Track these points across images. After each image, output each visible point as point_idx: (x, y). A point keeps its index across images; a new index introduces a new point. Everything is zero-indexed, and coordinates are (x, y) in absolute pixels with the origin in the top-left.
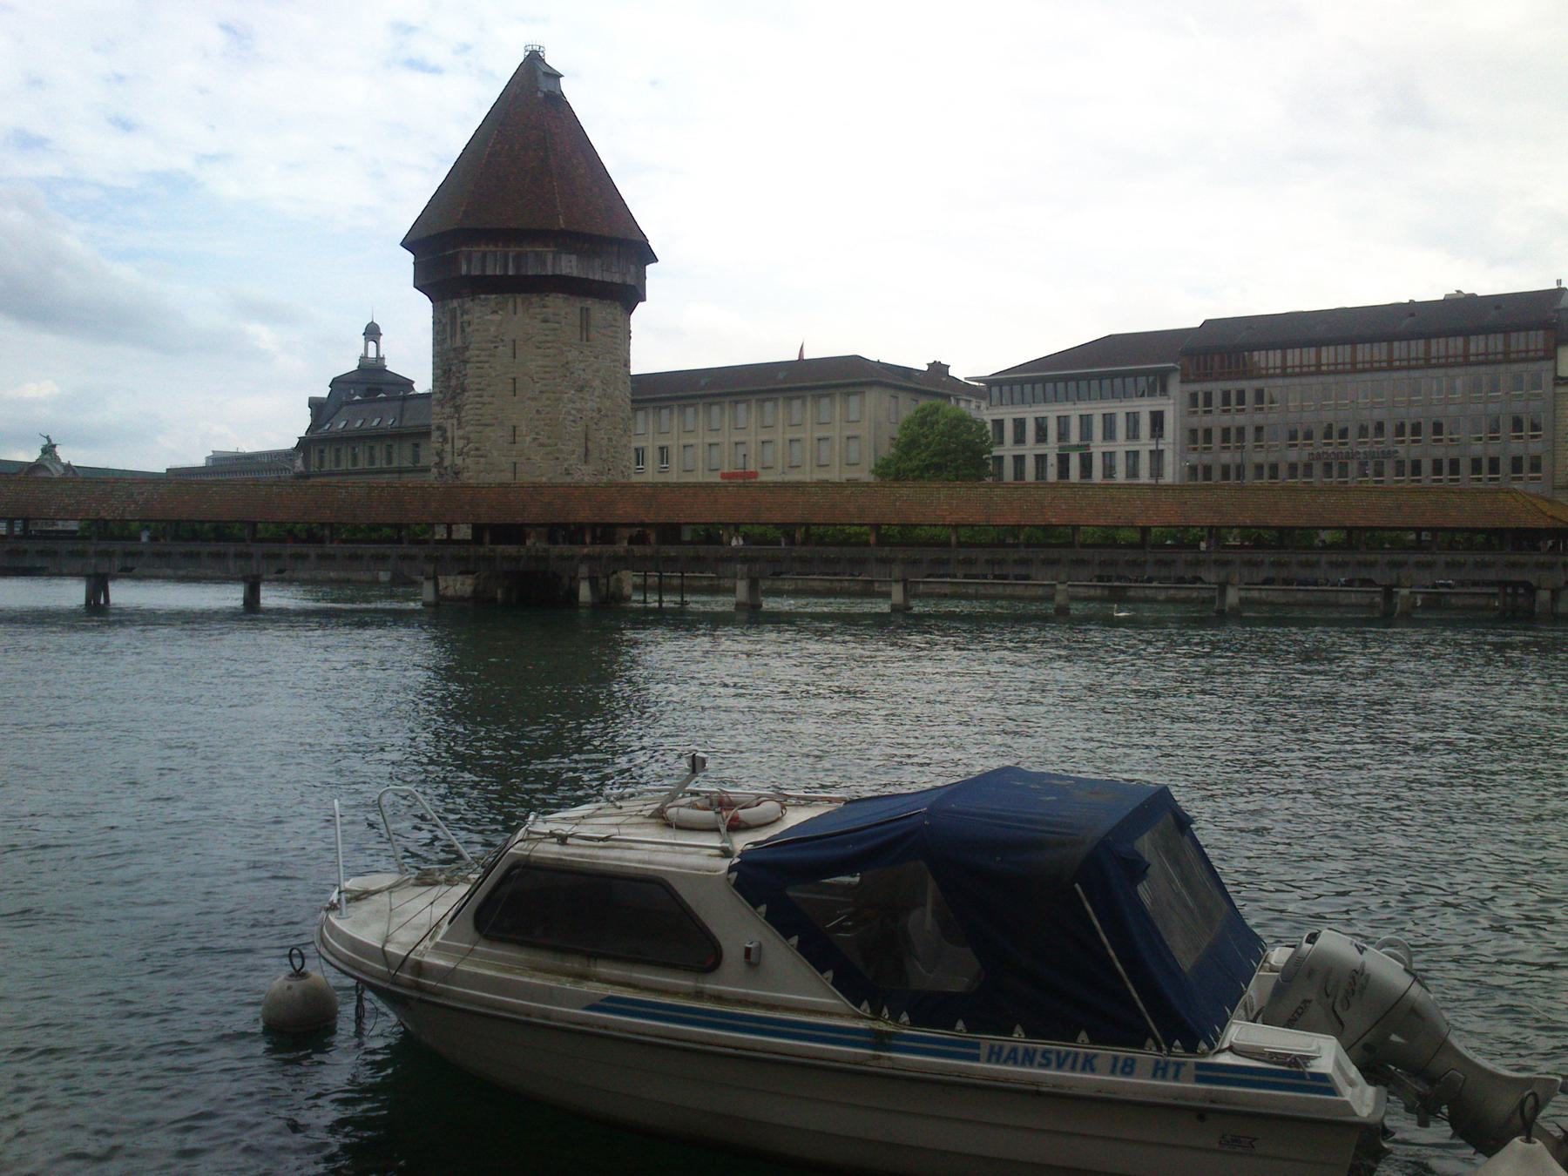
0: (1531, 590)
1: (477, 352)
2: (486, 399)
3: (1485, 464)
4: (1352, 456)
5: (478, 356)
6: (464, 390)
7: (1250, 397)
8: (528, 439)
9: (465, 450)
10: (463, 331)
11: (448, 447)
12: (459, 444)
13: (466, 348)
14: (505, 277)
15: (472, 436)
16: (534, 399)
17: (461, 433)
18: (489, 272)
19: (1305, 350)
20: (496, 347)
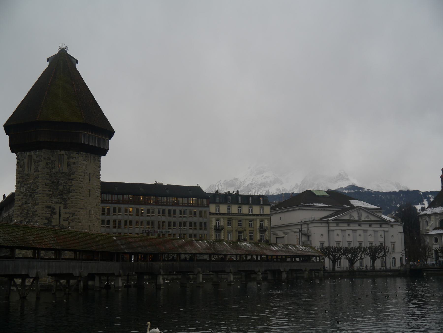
0: (280, 273)
1: (80, 176)
2: (82, 197)
3: (193, 236)
4: (155, 232)
5: (80, 178)
6: (69, 192)
7: (123, 210)
8: (94, 216)
9: (70, 219)
10: (69, 165)
12: (67, 216)
13: (73, 174)
14: (95, 146)
15: (76, 213)
16: (95, 199)
18: (90, 144)
19: (107, 195)
20: (85, 175)
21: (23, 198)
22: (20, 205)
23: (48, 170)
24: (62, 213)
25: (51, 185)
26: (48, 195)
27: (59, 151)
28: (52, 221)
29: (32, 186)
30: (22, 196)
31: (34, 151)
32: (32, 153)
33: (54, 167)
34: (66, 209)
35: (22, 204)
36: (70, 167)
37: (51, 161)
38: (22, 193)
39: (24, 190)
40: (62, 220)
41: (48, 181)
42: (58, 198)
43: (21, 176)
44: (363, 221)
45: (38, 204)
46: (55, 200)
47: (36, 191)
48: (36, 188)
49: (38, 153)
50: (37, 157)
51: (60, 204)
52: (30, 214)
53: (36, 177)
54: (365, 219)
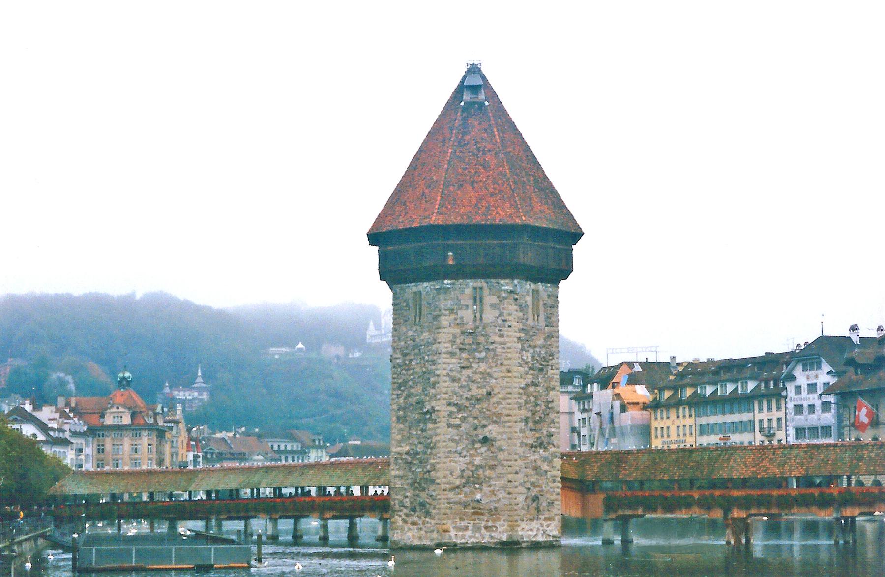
21: (527, 374)
22: (522, 385)
30: (526, 369)
31: (543, 284)
32: (540, 286)
35: (527, 385)
38: (527, 363)
39: (530, 359)
43: (523, 329)
47: (550, 363)
48: (550, 358)
50: (549, 296)
53: (548, 336)
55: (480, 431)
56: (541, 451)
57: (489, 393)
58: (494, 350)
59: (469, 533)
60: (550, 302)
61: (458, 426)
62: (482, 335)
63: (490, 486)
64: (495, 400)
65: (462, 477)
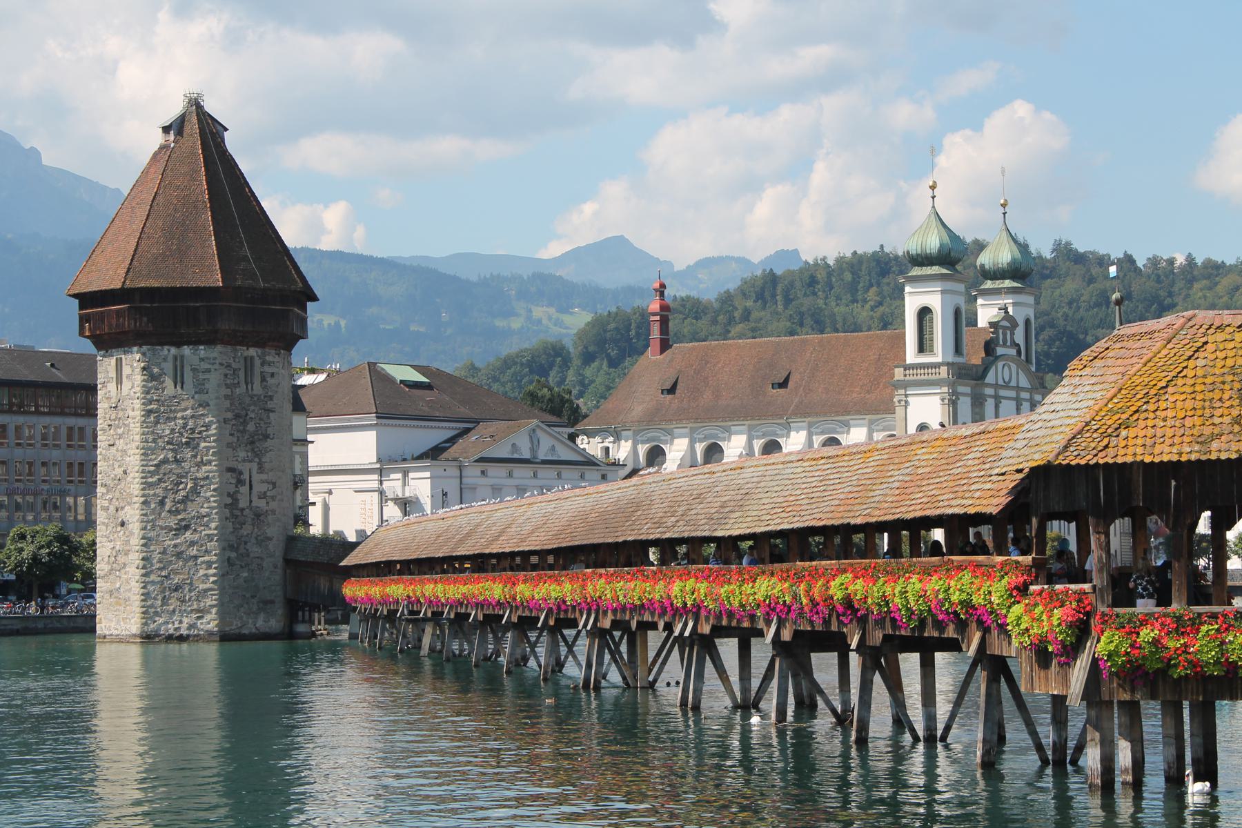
6: (266, 437)
10: (263, 379)
11: (244, 489)
13: (271, 398)
17: (264, 477)
21: (164, 448)
23: (229, 392)
24: (254, 483)
25: (234, 422)
26: (229, 445)
27: (245, 348)
28: (238, 500)
29: (191, 424)
31: (191, 347)
32: (186, 350)
33: (238, 383)
34: (261, 473)
35: (165, 461)
36: (265, 383)
37: (232, 372)
39: (167, 432)
40: (255, 499)
41: (229, 415)
42: (247, 451)
44: (544, 462)
45: (210, 462)
46: (242, 454)
48: (203, 429)
49: (202, 352)
51: (250, 461)
52: (187, 484)
54: (545, 456)
55: (119, 512)
56: (188, 534)
57: (125, 472)
58: (128, 425)
59: (113, 625)
60: (205, 366)
61: (107, 509)
62: (122, 409)
63: (125, 574)
64: (129, 479)
65: (108, 563)
